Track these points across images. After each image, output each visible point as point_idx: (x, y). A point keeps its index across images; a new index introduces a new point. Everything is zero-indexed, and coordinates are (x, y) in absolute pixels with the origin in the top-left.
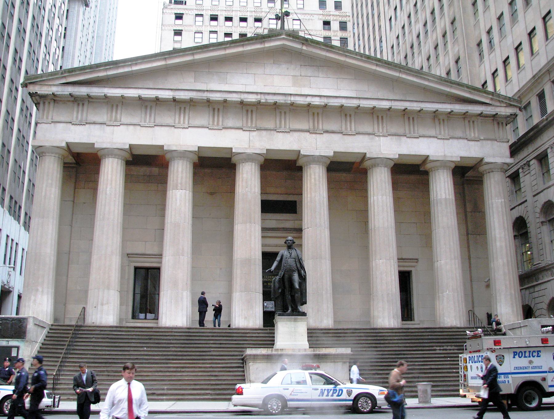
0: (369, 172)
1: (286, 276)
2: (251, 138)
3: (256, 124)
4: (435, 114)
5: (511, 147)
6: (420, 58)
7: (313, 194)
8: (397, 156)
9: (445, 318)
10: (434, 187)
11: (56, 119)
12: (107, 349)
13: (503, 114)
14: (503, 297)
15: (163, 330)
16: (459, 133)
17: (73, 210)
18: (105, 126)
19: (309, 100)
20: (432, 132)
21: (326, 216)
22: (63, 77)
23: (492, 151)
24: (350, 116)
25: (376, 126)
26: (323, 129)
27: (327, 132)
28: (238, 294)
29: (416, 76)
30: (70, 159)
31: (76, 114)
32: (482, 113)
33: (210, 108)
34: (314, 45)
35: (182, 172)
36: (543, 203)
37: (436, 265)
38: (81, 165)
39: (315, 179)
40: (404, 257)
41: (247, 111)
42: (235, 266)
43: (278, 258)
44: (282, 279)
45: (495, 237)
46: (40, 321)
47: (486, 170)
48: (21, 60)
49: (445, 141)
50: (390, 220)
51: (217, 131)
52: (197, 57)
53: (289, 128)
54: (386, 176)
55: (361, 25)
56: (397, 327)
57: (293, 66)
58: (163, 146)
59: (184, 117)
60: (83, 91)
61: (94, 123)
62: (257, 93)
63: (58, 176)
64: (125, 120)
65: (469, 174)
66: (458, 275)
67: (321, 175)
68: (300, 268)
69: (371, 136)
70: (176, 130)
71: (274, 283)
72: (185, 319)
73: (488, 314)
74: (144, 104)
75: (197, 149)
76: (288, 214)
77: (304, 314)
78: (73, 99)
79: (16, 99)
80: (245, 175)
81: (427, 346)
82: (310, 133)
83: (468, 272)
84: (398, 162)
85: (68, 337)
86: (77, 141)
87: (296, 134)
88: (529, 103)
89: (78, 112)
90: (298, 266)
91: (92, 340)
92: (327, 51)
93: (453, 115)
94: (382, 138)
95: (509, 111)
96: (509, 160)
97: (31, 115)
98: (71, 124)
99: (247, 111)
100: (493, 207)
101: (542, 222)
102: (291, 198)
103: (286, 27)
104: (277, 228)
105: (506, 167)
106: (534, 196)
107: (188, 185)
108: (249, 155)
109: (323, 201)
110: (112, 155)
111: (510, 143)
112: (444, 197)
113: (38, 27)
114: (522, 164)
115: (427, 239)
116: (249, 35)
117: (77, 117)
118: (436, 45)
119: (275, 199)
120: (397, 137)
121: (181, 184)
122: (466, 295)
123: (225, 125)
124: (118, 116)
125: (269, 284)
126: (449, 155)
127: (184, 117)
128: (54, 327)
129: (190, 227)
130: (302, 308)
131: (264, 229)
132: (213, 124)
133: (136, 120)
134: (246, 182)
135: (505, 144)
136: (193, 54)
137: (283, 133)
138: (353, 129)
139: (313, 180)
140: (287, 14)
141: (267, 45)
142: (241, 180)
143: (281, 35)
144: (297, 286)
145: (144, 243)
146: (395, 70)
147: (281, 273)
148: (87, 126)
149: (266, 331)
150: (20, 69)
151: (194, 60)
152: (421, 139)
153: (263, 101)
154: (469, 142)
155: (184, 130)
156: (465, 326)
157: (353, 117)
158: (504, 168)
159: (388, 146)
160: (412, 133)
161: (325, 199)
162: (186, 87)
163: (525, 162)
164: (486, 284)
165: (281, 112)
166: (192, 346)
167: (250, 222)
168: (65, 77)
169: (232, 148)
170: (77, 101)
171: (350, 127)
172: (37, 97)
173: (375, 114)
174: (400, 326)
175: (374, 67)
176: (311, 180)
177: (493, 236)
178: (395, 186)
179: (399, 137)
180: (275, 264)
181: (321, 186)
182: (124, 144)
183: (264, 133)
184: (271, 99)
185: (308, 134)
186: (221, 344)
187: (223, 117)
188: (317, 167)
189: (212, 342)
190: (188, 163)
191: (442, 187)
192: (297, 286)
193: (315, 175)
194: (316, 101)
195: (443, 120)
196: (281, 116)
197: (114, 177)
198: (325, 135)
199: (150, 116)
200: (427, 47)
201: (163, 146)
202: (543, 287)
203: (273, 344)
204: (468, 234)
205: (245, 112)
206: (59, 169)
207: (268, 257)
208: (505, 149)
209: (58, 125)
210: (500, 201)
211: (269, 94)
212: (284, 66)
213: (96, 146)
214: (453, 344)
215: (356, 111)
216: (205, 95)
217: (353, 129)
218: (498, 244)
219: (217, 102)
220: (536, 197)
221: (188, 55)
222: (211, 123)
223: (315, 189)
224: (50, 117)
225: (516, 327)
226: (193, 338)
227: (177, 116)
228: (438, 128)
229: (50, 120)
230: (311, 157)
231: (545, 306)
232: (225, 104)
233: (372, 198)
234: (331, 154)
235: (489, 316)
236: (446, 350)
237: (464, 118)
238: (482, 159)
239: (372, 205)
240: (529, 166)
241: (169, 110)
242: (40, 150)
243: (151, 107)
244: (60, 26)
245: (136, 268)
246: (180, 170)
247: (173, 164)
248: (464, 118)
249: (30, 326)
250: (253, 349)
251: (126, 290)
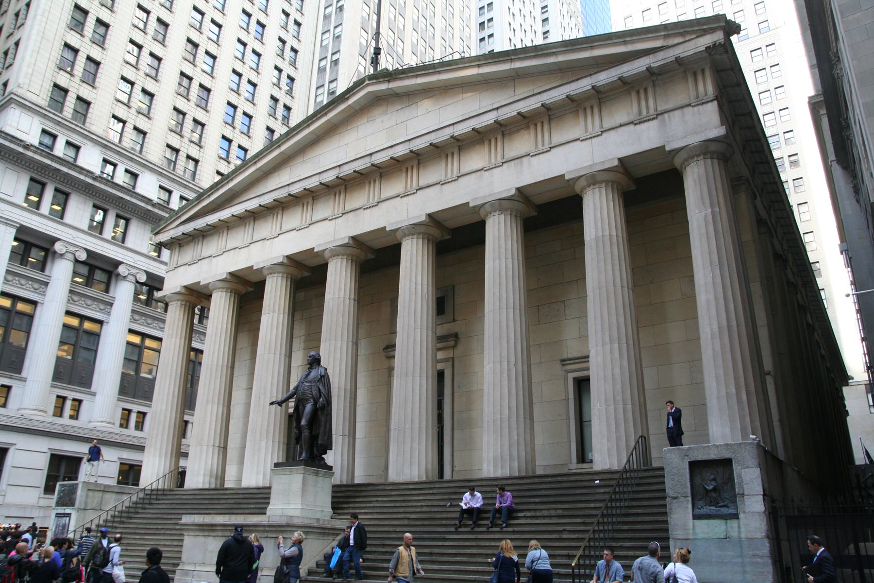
60: (189, 227)
66: (617, 371)
69: (479, 173)
112: (593, 236)
120: (516, 161)
135: (710, 104)
141: (351, 101)
154: (638, 127)
168: (180, 217)
185: (399, 198)
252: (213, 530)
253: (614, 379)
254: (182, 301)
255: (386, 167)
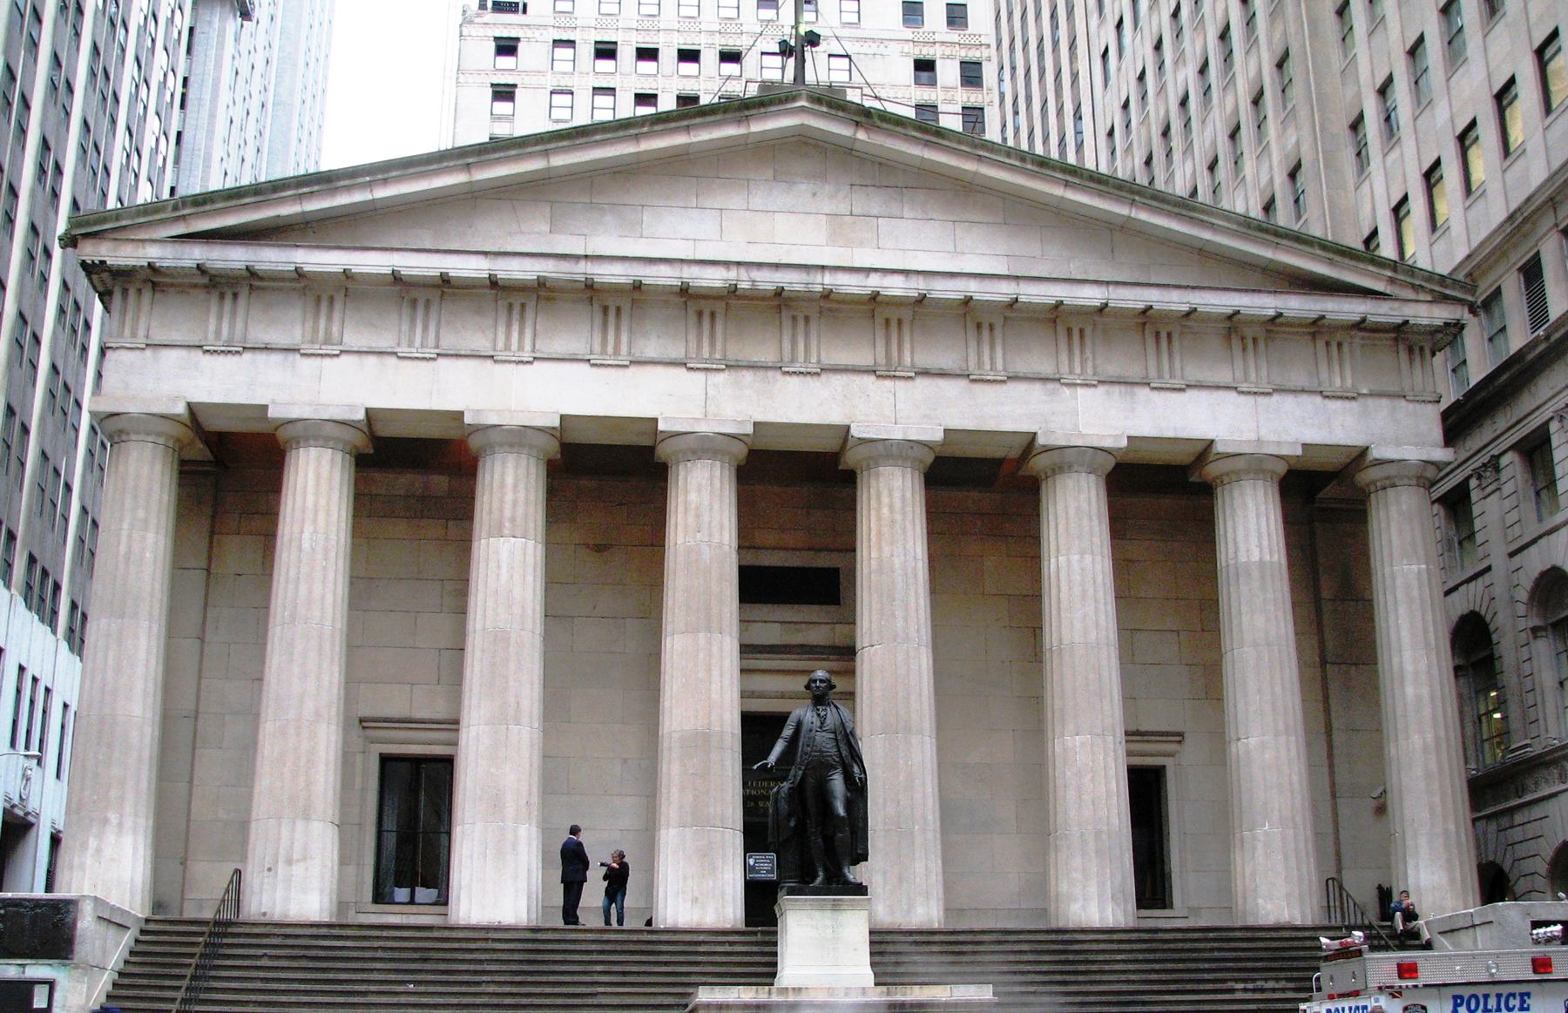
0: (1043, 486)
2: (711, 392)
3: (724, 351)
4: (1233, 324)
5: (1445, 415)
6: (1189, 165)
7: (886, 550)
8: (1124, 443)
9: (1260, 901)
10: (1230, 530)
11: (158, 338)
12: (302, 987)
13: (1425, 322)
14: (1423, 841)
15: (461, 935)
16: (1299, 378)
17: (207, 595)
18: (298, 356)
19: (874, 282)
20: (1224, 376)
21: (922, 612)
22: (178, 219)
23: (1394, 428)
24: (991, 328)
25: (1064, 357)
26: (913, 365)
27: (925, 373)
28: (672, 832)
29: (1178, 216)
30: (199, 451)
31: (214, 322)
32: (1364, 320)
33: (596, 306)
34: (890, 127)
35: (515, 487)
36: (1536, 574)
37: (1234, 749)
38: (229, 471)
39: (891, 507)
40: (1142, 729)
41: (700, 314)
42: (666, 753)
43: (788, 732)
44: (798, 791)
45: (1401, 669)
46: (113, 908)
47: (1374, 482)
48: (59, 170)
49: (1260, 399)
50: (1102, 622)
51: (613, 371)
52: (559, 161)
53: (819, 362)
54: (1094, 500)
55: (1020, 72)
56: (1123, 925)
57: (828, 189)
58: (462, 413)
59: (521, 332)
60: (235, 257)
61: (267, 349)
62: (726, 264)
63: (166, 497)
64: (353, 339)
65: (1329, 492)
66: (1295, 778)
67: (909, 495)
68: (848, 760)
69: (1050, 386)
70: (498, 367)
71: (776, 801)
72: (523, 904)
73: (1380, 887)
74: (407, 293)
75: (557, 423)
76: (816, 608)
77: (860, 890)
78: (205, 280)
79: (45, 280)
80: (693, 497)
81: (1209, 981)
82: (879, 377)
83: (1326, 769)
84: (1127, 459)
85: (192, 955)
86: (217, 398)
87: (838, 381)
88: (1497, 293)
89: (220, 318)
91: (259, 963)
92: (927, 144)
93: (1282, 325)
94: (1080, 391)
95: (1439, 314)
96: (1442, 454)
97: (88, 326)
98: (200, 352)
99: (700, 314)
100: (1394, 587)
101: (1535, 630)
102: (824, 561)
103: (810, 77)
104: (786, 646)
105: (1431, 473)
106: (1512, 555)
107: (532, 525)
108: (704, 438)
109: (915, 568)
110: (316, 438)
111: (1444, 405)
112: (1255, 557)
113: (107, 78)
114: (1479, 464)
115: (1208, 676)
116: (705, 100)
117: (218, 332)
118: (1233, 126)
119: (779, 564)
120: (1123, 388)
121: (513, 520)
122: (1318, 835)
123: (638, 355)
124: (335, 329)
125: (761, 804)
126: (1272, 438)
127: (521, 332)
128: (152, 927)
129: (538, 641)
130: (856, 873)
131: (746, 650)
132: (603, 352)
133: (384, 341)
134: (698, 516)
135: (1430, 406)
136: (546, 154)
137: (801, 378)
138: (999, 366)
139: (885, 511)
140: (813, 39)
141: (757, 127)
142: (681, 509)
143: (794, 99)
144: (841, 810)
145: (407, 688)
146: (1119, 200)
147: (796, 773)
148: (247, 356)
149: (753, 939)
150: (55, 195)
151: (548, 169)
152: (1191, 393)
153: (743, 285)
155: (521, 367)
156: (1318, 923)
157: (998, 333)
158: (1426, 476)
159: (1098, 414)
160: (1167, 376)
161: (920, 565)
162: (526, 246)
163: (1486, 459)
164: (1374, 803)
165: (794, 318)
166: (544, 979)
167: (709, 629)
169: (655, 420)
170: (218, 286)
171: (992, 359)
172: (105, 275)
173: (1060, 322)
174: (1131, 924)
175: (1059, 191)
176: (879, 510)
177: (1395, 668)
178: (1120, 526)
179: (1129, 388)
180: (779, 747)
181: (909, 527)
182: (352, 407)
183: (748, 376)
184: (768, 280)
185: (872, 378)
186: (624, 973)
187: (631, 331)
188: (897, 471)
189: (599, 968)
190: (533, 461)
191: (1252, 532)
192: (841, 810)
193: (891, 495)
194: (895, 287)
195: (1255, 340)
196: (794, 326)
197: (323, 502)
198: (921, 382)
199: (425, 328)
200: (1210, 133)
201: (462, 413)
202: (1537, 811)
203: (774, 975)
204: (1323, 662)
205: (692, 318)
206: (167, 480)
207: (758, 728)
208: (1428, 422)
209: (165, 353)
210: (1415, 568)
211: (760, 265)
212: (803, 187)
213: (272, 413)
214: (1282, 975)
215: (1008, 314)
216: (582, 270)
217: (999, 366)
218: (1410, 690)
219: (616, 290)
220: (1517, 558)
221: (531, 155)
222: (597, 347)
223: (892, 535)
224: (141, 333)
225: (1460, 925)
226: (547, 957)
227: (501, 330)
228: (1239, 363)
229: (141, 340)
230: (880, 446)
231: (1542, 866)
232: (637, 296)
233: (1053, 560)
234: (938, 436)
235: (1385, 895)
236: (1262, 990)
237: (1314, 336)
238: (1364, 451)
239: (1053, 580)
240: (1497, 469)
241: (479, 311)
242: (112, 425)
243: (428, 303)
244: (171, 74)
245: (385, 760)
246: (509, 480)
247: (488, 464)
248: (1314, 336)
249: (86, 923)
250: (717, 988)
251: (357, 821)
253: (1292, 792)
254: (169, 437)
255: (842, 302)
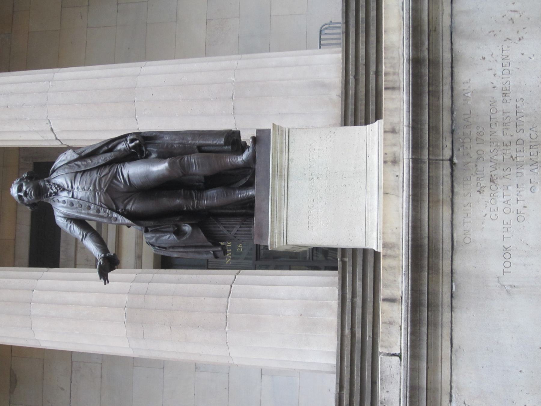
1: (131, 207)
68: (109, 156)
90: (100, 160)
252: (434, 251)
